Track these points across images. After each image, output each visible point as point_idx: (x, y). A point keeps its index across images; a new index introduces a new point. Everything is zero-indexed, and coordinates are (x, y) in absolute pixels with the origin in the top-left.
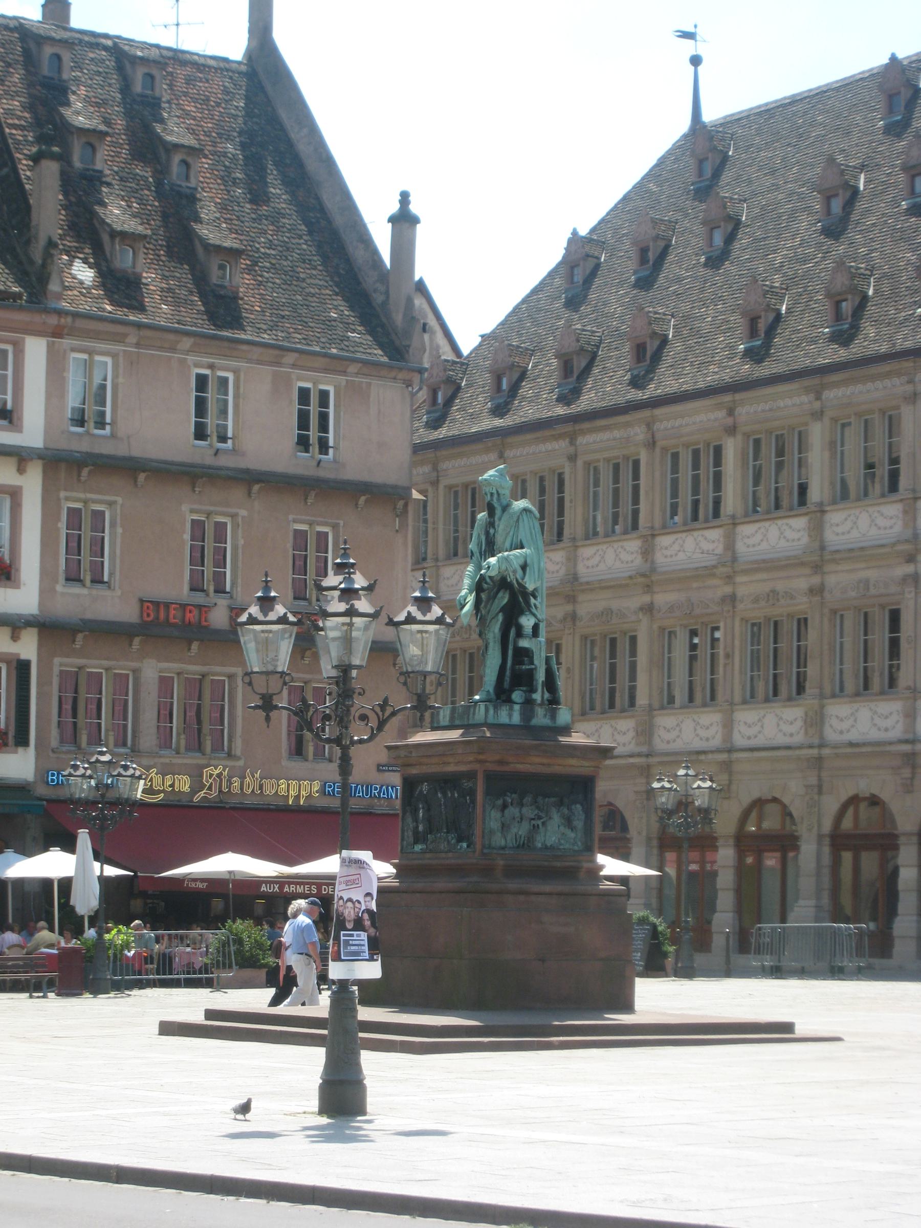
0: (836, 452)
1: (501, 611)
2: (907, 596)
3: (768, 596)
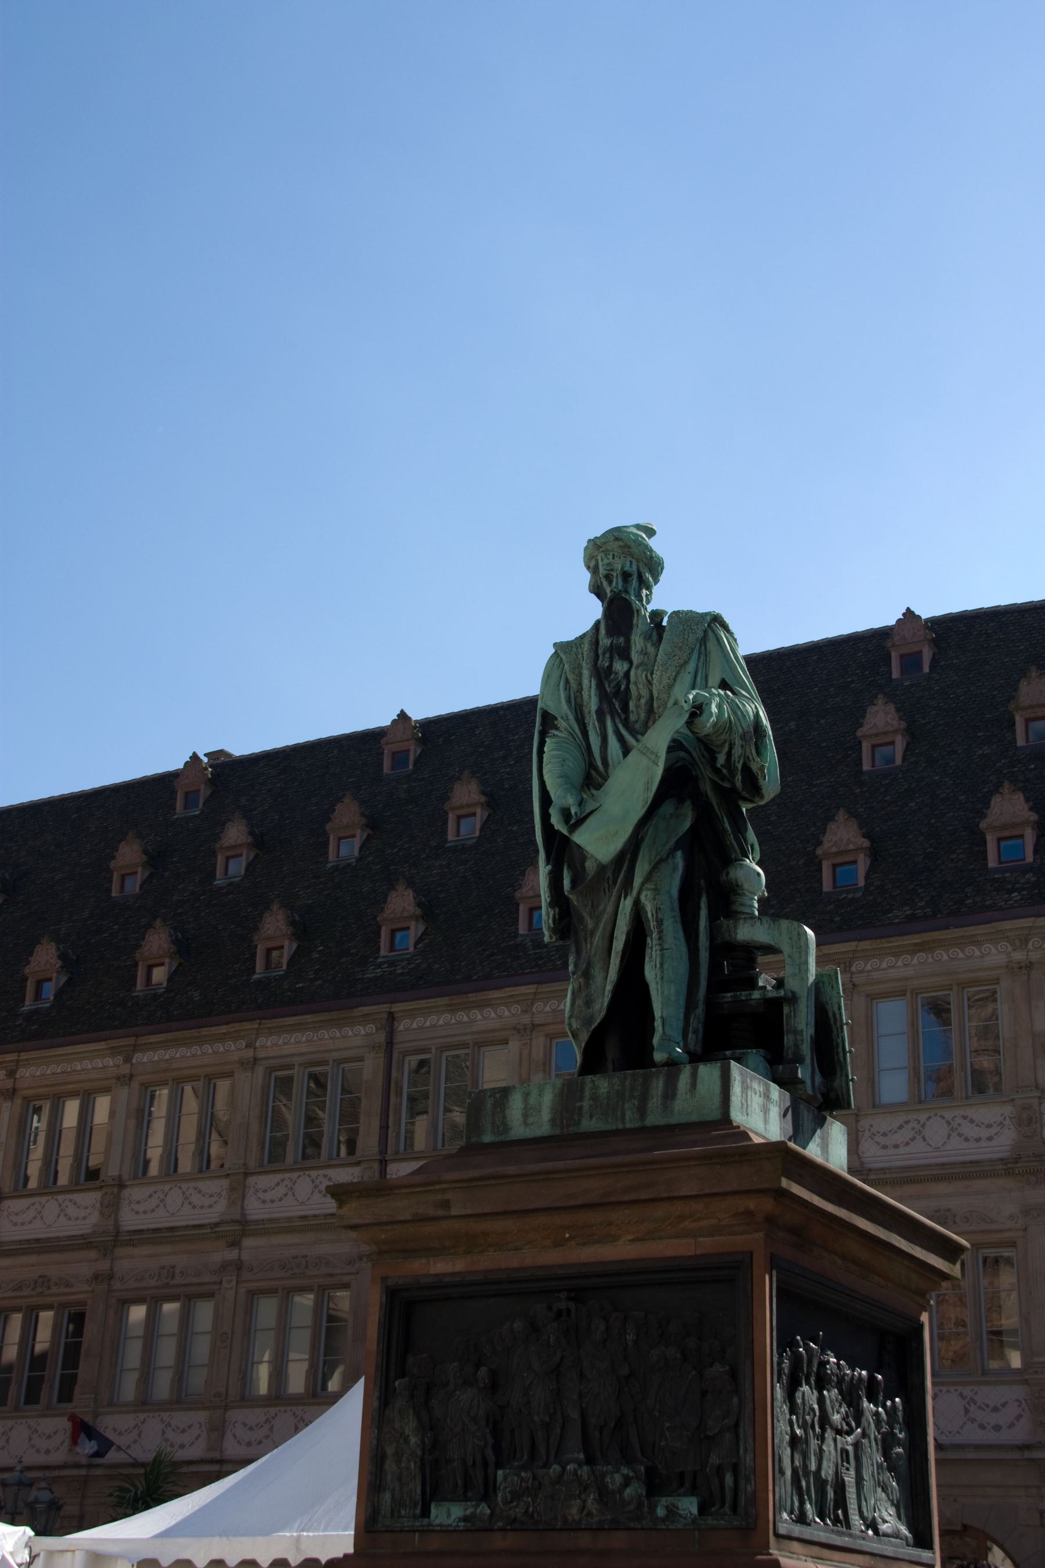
0: (143, 1121)
1: (678, 846)
2: (225, 1285)
3: (36, 1283)
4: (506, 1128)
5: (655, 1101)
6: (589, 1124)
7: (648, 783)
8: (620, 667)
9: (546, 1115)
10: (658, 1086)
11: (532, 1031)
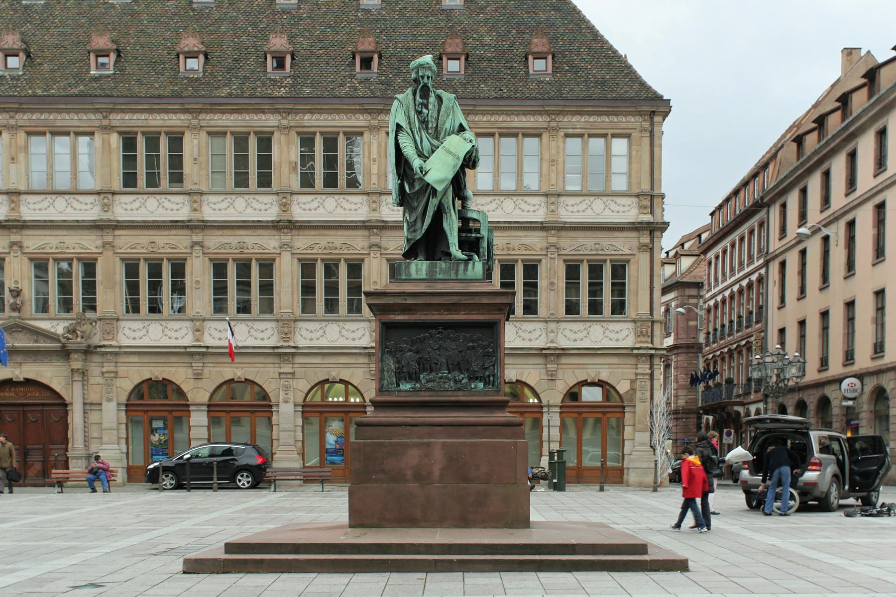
4: (410, 274)
5: (461, 271)
6: (439, 276)
7: (455, 166)
8: (425, 111)
9: (424, 272)
10: (462, 267)
11: (16, 129)
